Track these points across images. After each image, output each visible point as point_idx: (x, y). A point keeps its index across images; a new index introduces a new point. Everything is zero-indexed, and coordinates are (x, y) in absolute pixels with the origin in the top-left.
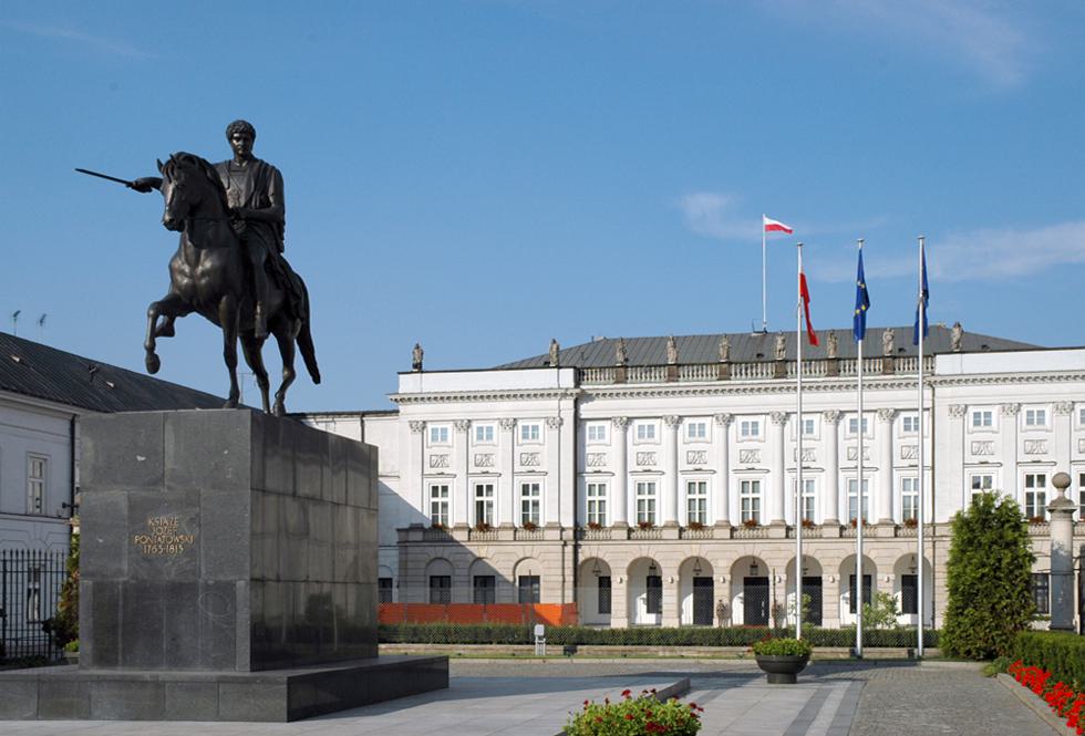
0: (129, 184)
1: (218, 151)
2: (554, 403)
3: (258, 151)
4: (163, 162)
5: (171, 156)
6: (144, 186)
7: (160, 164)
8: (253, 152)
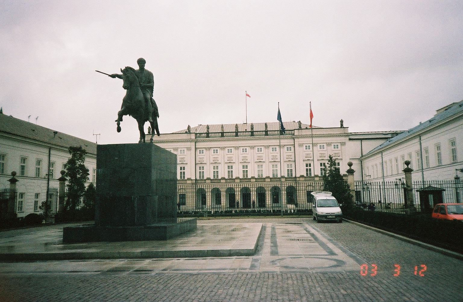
0: (109, 76)
1: (136, 67)
2: (189, 143)
3: (147, 67)
4: (123, 69)
5: (125, 67)
6: (113, 76)
7: (122, 71)
8: (145, 68)
